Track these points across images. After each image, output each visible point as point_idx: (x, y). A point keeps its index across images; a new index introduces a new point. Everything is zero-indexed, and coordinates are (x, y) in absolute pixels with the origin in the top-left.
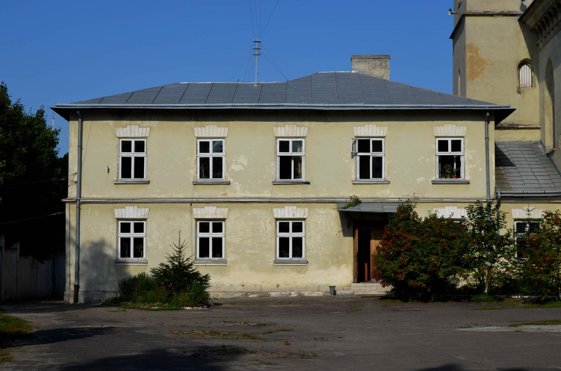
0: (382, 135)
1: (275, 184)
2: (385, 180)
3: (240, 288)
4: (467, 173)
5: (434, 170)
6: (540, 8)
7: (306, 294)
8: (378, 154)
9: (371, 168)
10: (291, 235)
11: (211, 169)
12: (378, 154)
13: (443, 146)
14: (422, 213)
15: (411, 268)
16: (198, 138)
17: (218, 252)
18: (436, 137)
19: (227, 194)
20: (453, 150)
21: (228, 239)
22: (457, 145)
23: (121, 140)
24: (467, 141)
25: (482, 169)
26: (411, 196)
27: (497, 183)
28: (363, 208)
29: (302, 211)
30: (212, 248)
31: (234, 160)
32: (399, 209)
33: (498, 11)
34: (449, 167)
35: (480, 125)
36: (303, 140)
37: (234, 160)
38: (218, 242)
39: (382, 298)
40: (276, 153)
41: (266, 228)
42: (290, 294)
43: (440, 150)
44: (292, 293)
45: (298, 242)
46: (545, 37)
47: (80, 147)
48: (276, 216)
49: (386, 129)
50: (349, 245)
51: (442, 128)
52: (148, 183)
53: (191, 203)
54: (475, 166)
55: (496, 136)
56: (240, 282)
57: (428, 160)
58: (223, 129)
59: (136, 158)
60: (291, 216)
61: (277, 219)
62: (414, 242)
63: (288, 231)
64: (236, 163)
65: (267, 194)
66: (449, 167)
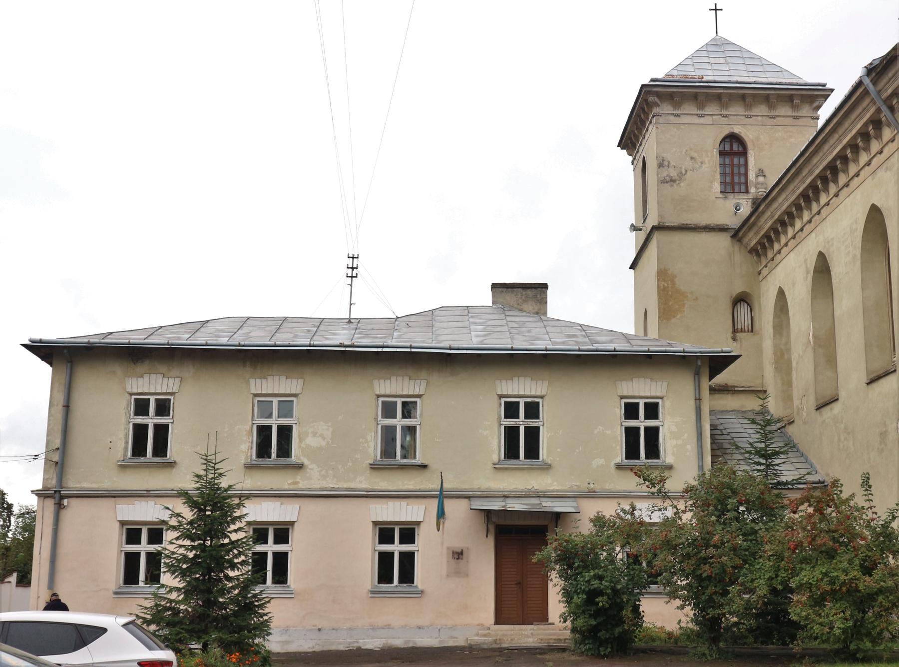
0: (539, 393)
1: (374, 467)
5: (618, 448)
6: (768, 214)
8: (532, 423)
9: (522, 444)
10: (396, 548)
13: (631, 411)
16: (256, 395)
18: (622, 398)
19: (297, 483)
20: (647, 417)
22: (652, 411)
23: (134, 397)
25: (691, 447)
31: (310, 430)
34: (641, 445)
36: (418, 400)
37: (310, 430)
40: (376, 419)
46: (773, 259)
49: (546, 383)
51: (630, 383)
54: (680, 442)
57: (609, 432)
58: (294, 381)
59: (156, 426)
64: (314, 434)
66: (641, 445)
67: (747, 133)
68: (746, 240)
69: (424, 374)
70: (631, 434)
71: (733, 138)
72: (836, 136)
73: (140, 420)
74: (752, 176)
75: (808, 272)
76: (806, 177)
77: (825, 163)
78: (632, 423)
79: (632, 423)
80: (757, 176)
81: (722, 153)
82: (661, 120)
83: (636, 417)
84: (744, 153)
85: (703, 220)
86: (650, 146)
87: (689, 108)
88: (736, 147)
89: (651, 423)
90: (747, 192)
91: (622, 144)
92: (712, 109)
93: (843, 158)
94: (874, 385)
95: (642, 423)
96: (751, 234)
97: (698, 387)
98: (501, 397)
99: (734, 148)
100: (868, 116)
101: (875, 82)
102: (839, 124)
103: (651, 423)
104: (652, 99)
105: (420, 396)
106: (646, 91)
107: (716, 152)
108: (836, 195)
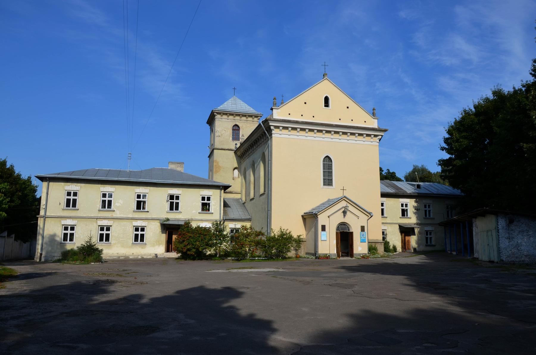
3: (116, 255)
7: (145, 257)
8: (177, 201)
9: (174, 206)
10: (140, 233)
11: (107, 204)
12: (177, 201)
13: (203, 199)
14: (194, 225)
15: (189, 247)
17: (107, 239)
21: (113, 234)
22: (209, 199)
25: (218, 208)
26: (190, 218)
28: (170, 223)
30: (105, 238)
32: (185, 223)
33: (227, 148)
34: (205, 207)
35: (218, 191)
38: (108, 236)
39: (177, 259)
45: (142, 236)
47: (47, 193)
50: (164, 237)
52: (78, 210)
53: (97, 219)
55: (224, 195)
56: (117, 252)
59: (73, 199)
62: (190, 236)
65: (130, 216)
66: (205, 207)
71: (236, 125)
73: (69, 197)
74: (240, 136)
81: (233, 130)
84: (239, 130)
88: (237, 128)
91: (207, 123)
92: (231, 117)
99: (236, 129)
104: (215, 114)
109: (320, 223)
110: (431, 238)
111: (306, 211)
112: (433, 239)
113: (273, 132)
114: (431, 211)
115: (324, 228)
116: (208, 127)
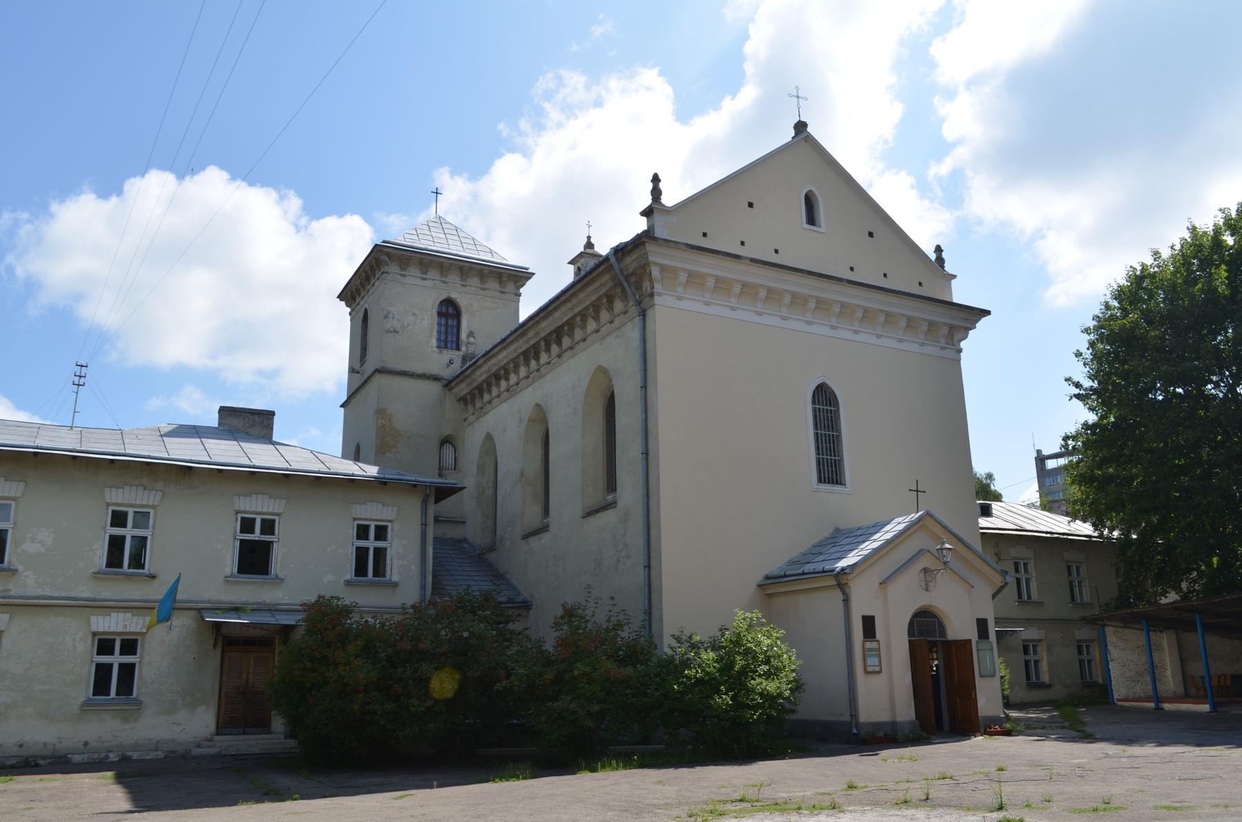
1: (97, 575)
2: (277, 577)
4: (395, 571)
7: (135, 756)
9: (254, 559)
13: (362, 532)
19: (9, 590)
22: (381, 533)
24: (396, 527)
25: (415, 568)
27: (433, 589)
29: (141, 622)
31: (29, 535)
37: (29, 535)
40: (104, 528)
41: (75, 648)
42: (107, 757)
43: (359, 537)
44: (111, 755)
45: (128, 671)
48: (94, 628)
49: (284, 502)
58: (15, 484)
60: (120, 629)
61: (94, 634)
63: (112, 653)
65: (84, 591)
67: (462, 299)
68: (456, 390)
69: (160, 485)
70: (361, 554)
72: (569, 305)
74: (463, 336)
75: (521, 420)
76: (530, 339)
77: (553, 328)
78: (362, 543)
79: (362, 543)
80: (468, 336)
81: (440, 314)
82: (389, 277)
83: (367, 538)
85: (420, 370)
86: (367, 302)
87: (414, 271)
88: (450, 310)
89: (380, 544)
90: (458, 348)
91: (341, 297)
92: (433, 274)
93: (570, 324)
94: (591, 519)
95: (371, 544)
96: (463, 385)
97: (424, 513)
98: (237, 512)
99: (450, 312)
100: (604, 290)
101: (619, 260)
102: (574, 295)
103: (380, 544)
105: (153, 507)
106: (377, 249)
107: (435, 312)
108: (559, 356)
109: (858, 612)
110: (1036, 662)
111: (767, 572)
112: (1044, 666)
113: (658, 287)
114: (1033, 584)
115: (869, 624)
116: (344, 310)
